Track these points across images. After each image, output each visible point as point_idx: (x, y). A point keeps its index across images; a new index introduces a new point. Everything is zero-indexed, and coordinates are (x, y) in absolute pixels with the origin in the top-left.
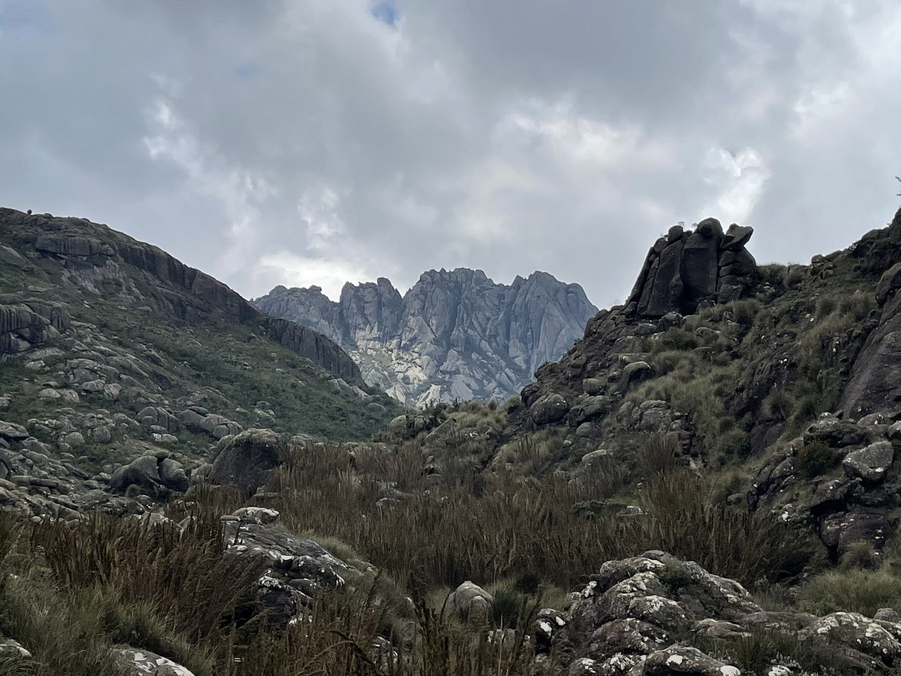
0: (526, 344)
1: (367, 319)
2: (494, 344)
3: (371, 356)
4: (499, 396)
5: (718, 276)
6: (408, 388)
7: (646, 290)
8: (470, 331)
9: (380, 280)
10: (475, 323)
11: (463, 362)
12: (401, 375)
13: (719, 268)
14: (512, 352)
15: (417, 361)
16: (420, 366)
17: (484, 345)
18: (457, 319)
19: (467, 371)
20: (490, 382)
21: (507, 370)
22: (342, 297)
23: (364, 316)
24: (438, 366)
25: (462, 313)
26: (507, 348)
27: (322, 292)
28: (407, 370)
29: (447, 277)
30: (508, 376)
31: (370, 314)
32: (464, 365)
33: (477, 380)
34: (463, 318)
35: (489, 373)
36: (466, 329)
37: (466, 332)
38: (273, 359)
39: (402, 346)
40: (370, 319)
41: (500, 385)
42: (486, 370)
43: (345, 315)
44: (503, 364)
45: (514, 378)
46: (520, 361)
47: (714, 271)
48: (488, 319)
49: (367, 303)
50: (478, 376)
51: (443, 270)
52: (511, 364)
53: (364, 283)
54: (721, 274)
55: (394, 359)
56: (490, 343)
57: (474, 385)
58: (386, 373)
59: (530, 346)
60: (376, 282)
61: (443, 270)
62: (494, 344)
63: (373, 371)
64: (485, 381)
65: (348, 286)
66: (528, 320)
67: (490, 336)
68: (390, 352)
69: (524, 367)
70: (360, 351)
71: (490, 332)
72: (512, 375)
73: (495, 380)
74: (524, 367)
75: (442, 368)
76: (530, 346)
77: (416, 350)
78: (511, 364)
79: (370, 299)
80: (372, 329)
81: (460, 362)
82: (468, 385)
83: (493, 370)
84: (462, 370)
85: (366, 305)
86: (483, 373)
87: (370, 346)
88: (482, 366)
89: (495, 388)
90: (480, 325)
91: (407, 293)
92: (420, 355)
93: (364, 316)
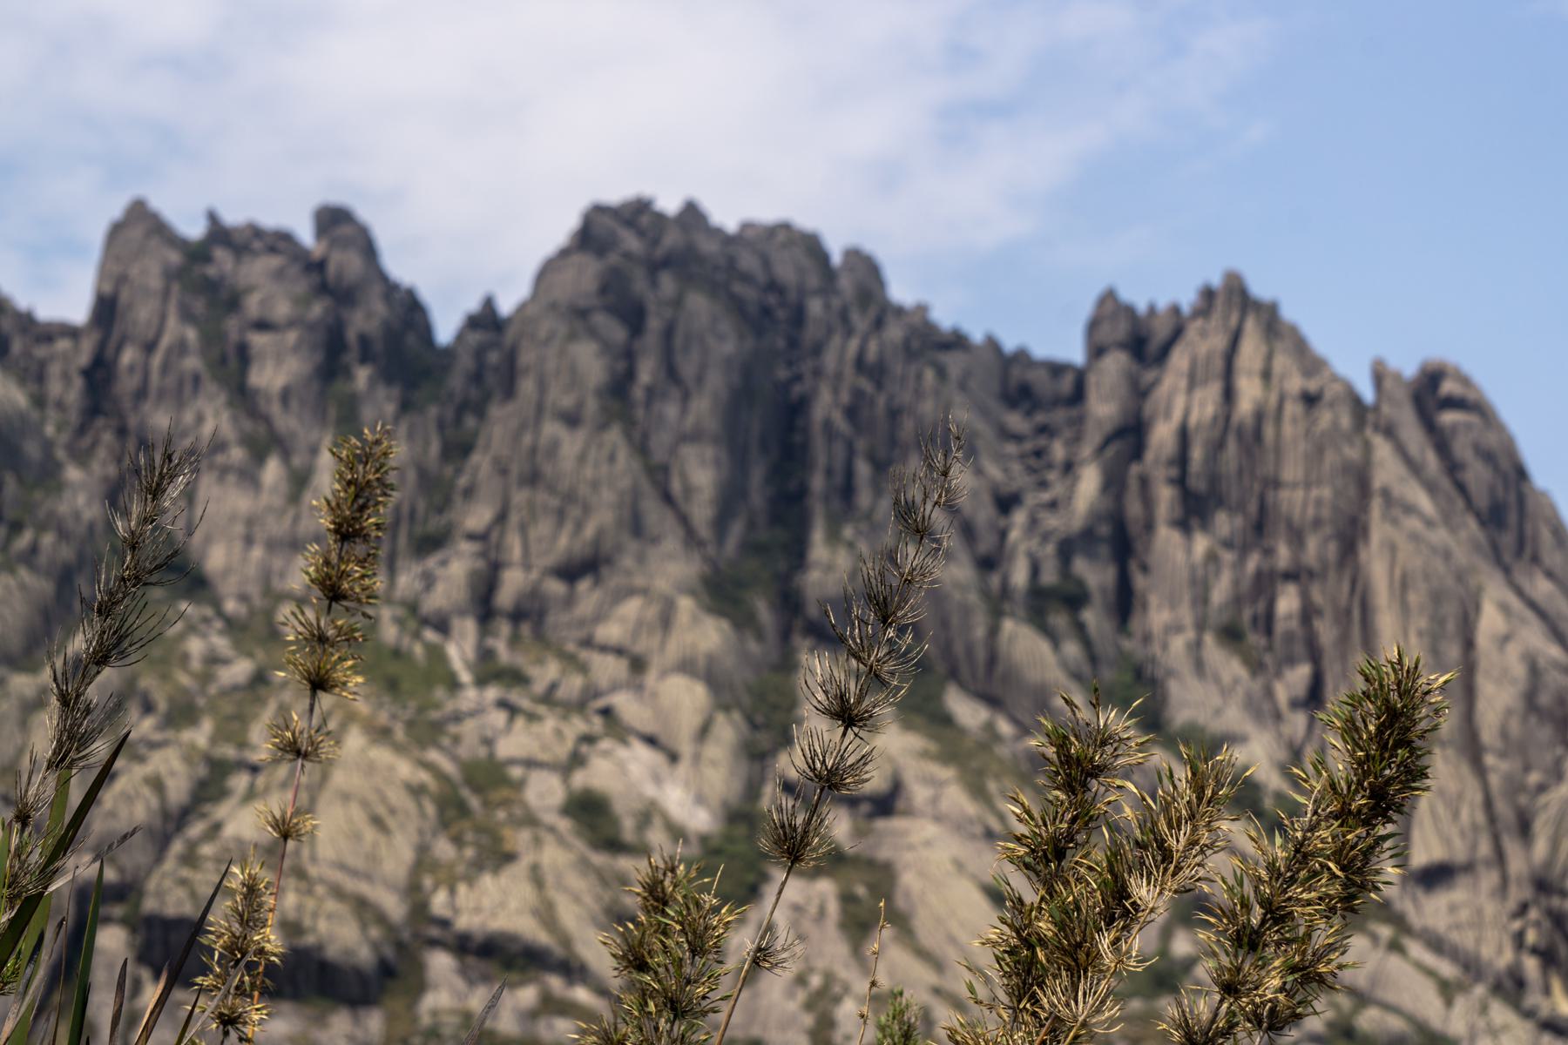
12: (545, 792)
16: (651, 741)
19: (956, 798)
24: (756, 755)
28: (577, 760)
31: (285, 395)
39: (506, 596)
40: (285, 422)
43: (126, 384)
48: (1006, 503)
49: (263, 325)
59: (1300, 674)
60: (306, 235)
63: (355, 740)
68: (430, 635)
77: (611, 631)
79: (282, 309)
84: (919, 794)
85: (258, 340)
92: (638, 665)
93: (243, 397)
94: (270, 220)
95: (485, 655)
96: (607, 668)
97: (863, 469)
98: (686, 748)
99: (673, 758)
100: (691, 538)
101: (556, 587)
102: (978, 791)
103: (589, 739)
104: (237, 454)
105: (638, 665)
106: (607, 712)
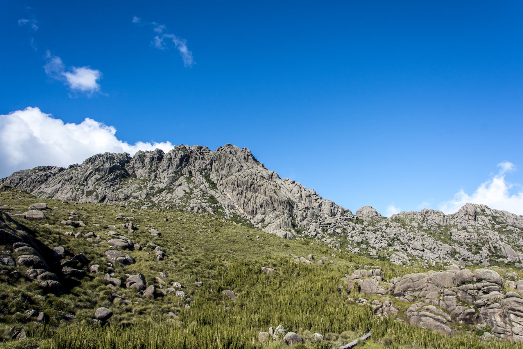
6: (151, 192)
14: (211, 177)
16: (163, 183)
19: (186, 184)
29: (187, 148)
32: (186, 182)
33: (190, 188)
44: (204, 180)
50: (191, 187)
57: (188, 190)
58: (142, 186)
62: (203, 174)
64: (194, 189)
67: (202, 169)
69: (215, 182)
75: (174, 183)
80: (146, 168)
81: (185, 180)
82: (184, 191)
84: (183, 184)
86: (194, 185)
87: (143, 176)
101: (161, 173)
102: (188, 184)
104: (141, 167)
105: (165, 178)
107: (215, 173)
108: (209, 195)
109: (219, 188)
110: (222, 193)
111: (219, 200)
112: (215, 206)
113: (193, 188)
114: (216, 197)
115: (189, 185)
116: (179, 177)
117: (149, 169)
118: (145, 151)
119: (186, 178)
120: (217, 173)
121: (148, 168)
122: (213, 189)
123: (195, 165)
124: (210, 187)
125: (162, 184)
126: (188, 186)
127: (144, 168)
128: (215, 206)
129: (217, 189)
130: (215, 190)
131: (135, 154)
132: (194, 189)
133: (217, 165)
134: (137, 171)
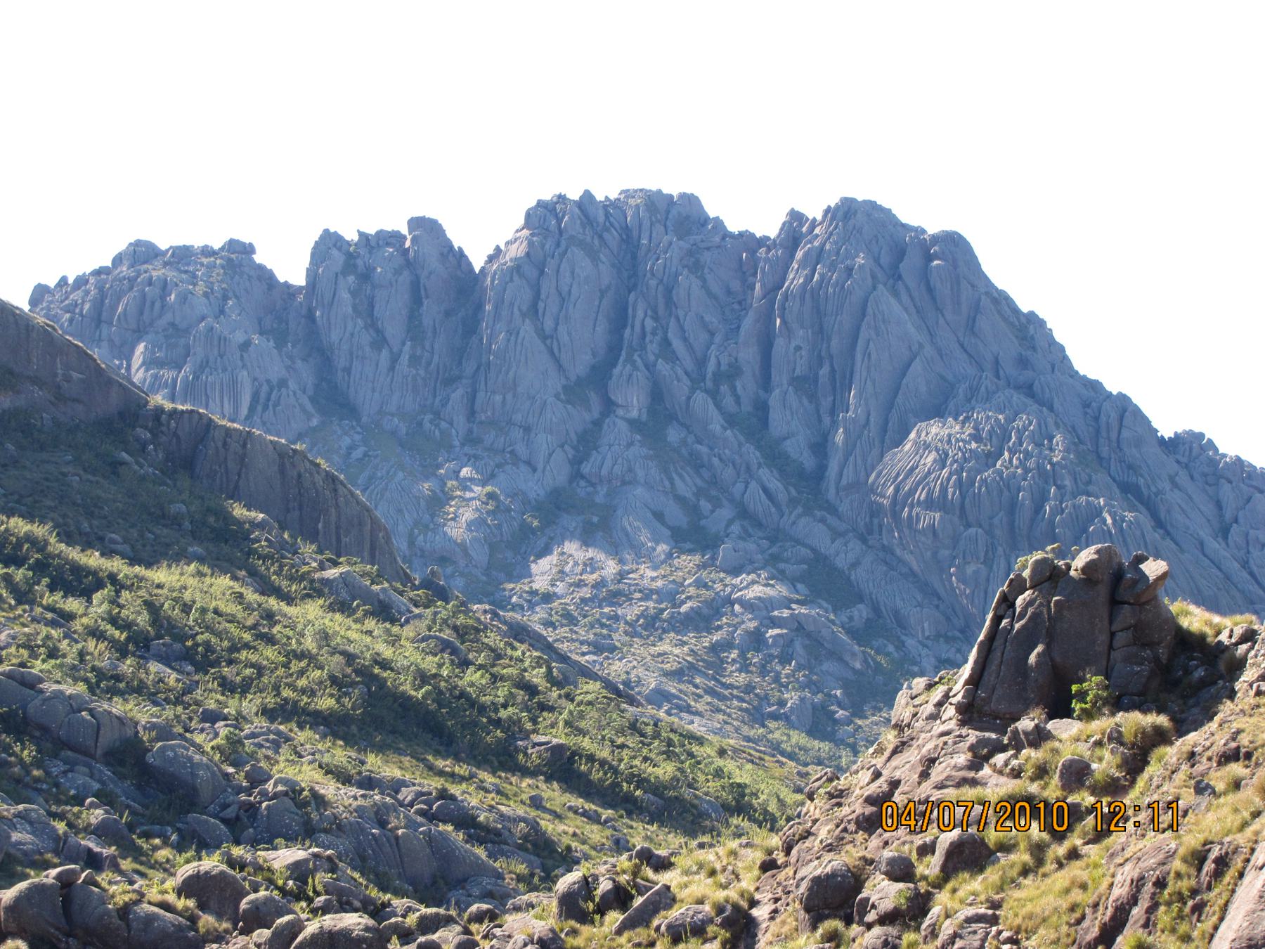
0: (813, 397)
1: (379, 332)
2: (728, 402)
3: (393, 433)
4: (741, 544)
5: (1111, 647)
7: (993, 667)
8: (663, 367)
9: (417, 223)
10: (677, 344)
11: (644, 451)
13: (1113, 634)
15: (521, 449)
16: (529, 463)
17: (701, 400)
18: (627, 332)
20: (717, 504)
21: (766, 475)
22: (312, 274)
23: (372, 323)
24: (577, 462)
25: (640, 314)
26: (762, 409)
27: (258, 258)
30: (765, 490)
33: (680, 499)
34: (643, 327)
35: (714, 482)
36: (652, 358)
37: (649, 367)
38: (176, 522)
41: (744, 513)
42: (706, 474)
44: (752, 454)
45: (782, 497)
46: (798, 449)
47: (1103, 638)
50: (684, 489)
51: (587, 195)
52: (775, 457)
53: (371, 231)
54: (1116, 644)
55: (457, 443)
56: (714, 395)
57: (677, 515)
59: (826, 403)
60: (404, 230)
61: (587, 195)
65: (329, 244)
66: (821, 333)
67: (718, 377)
69: (809, 462)
70: (364, 419)
71: (719, 364)
72: (775, 484)
73: (732, 501)
74: (809, 462)
75: (586, 468)
76: (826, 403)
78: (775, 457)
80: (395, 359)
81: (636, 450)
83: (728, 473)
84: (640, 474)
86: (699, 482)
88: (697, 464)
89: (730, 522)
90: (690, 348)
91: (491, 259)
92: (527, 429)
93: (372, 323)
94: (389, 227)
95: (470, 431)
96: (517, 434)
97: (649, 323)
98: (540, 466)
99: (535, 470)
100: (560, 367)
103: (498, 466)
105: (527, 429)
106: (512, 452)
107: (792, 397)
108: (804, 552)
109: (843, 508)
110: (864, 540)
111: (859, 575)
112: (851, 618)
113: (699, 493)
114: (841, 562)
115: (671, 480)
116: (598, 424)
117: (414, 360)
118: (351, 235)
119: (634, 424)
120: (805, 401)
121: (405, 358)
122: (808, 511)
123: (666, 342)
124: (793, 502)
125: (524, 468)
126: (667, 483)
127: (385, 354)
128: (851, 618)
129: (832, 510)
130: (823, 521)
131: (305, 261)
132: (705, 505)
133: (798, 348)
134: (348, 370)
